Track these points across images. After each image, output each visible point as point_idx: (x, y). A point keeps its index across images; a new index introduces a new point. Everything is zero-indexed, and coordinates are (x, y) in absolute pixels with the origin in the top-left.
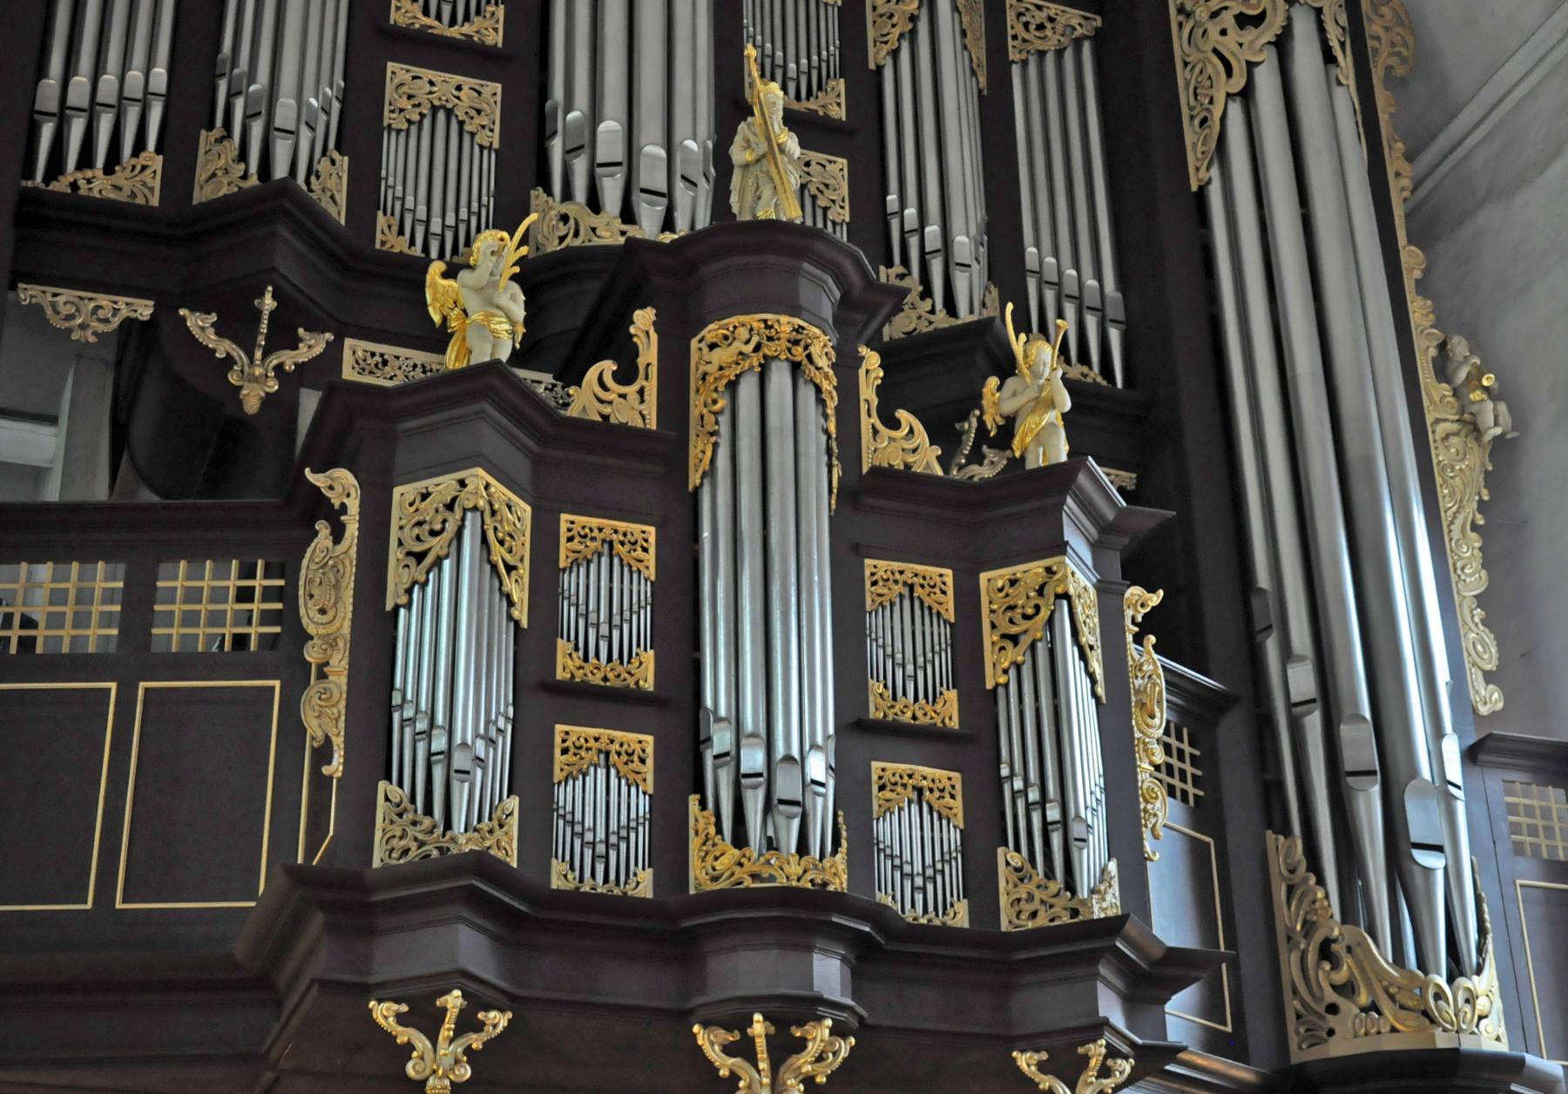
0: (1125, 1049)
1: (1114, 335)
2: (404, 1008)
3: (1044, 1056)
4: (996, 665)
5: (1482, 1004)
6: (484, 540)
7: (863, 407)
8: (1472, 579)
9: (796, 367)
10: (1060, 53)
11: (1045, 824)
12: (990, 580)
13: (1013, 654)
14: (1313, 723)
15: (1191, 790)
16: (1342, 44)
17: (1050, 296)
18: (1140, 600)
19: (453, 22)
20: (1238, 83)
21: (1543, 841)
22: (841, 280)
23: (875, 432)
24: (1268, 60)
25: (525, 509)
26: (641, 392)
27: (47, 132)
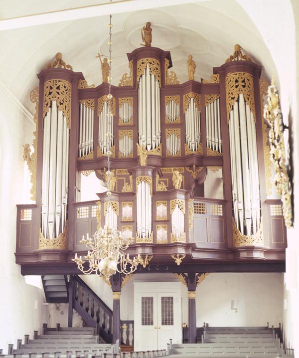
16: (248, 98)
24: (236, 103)
25: (118, 203)
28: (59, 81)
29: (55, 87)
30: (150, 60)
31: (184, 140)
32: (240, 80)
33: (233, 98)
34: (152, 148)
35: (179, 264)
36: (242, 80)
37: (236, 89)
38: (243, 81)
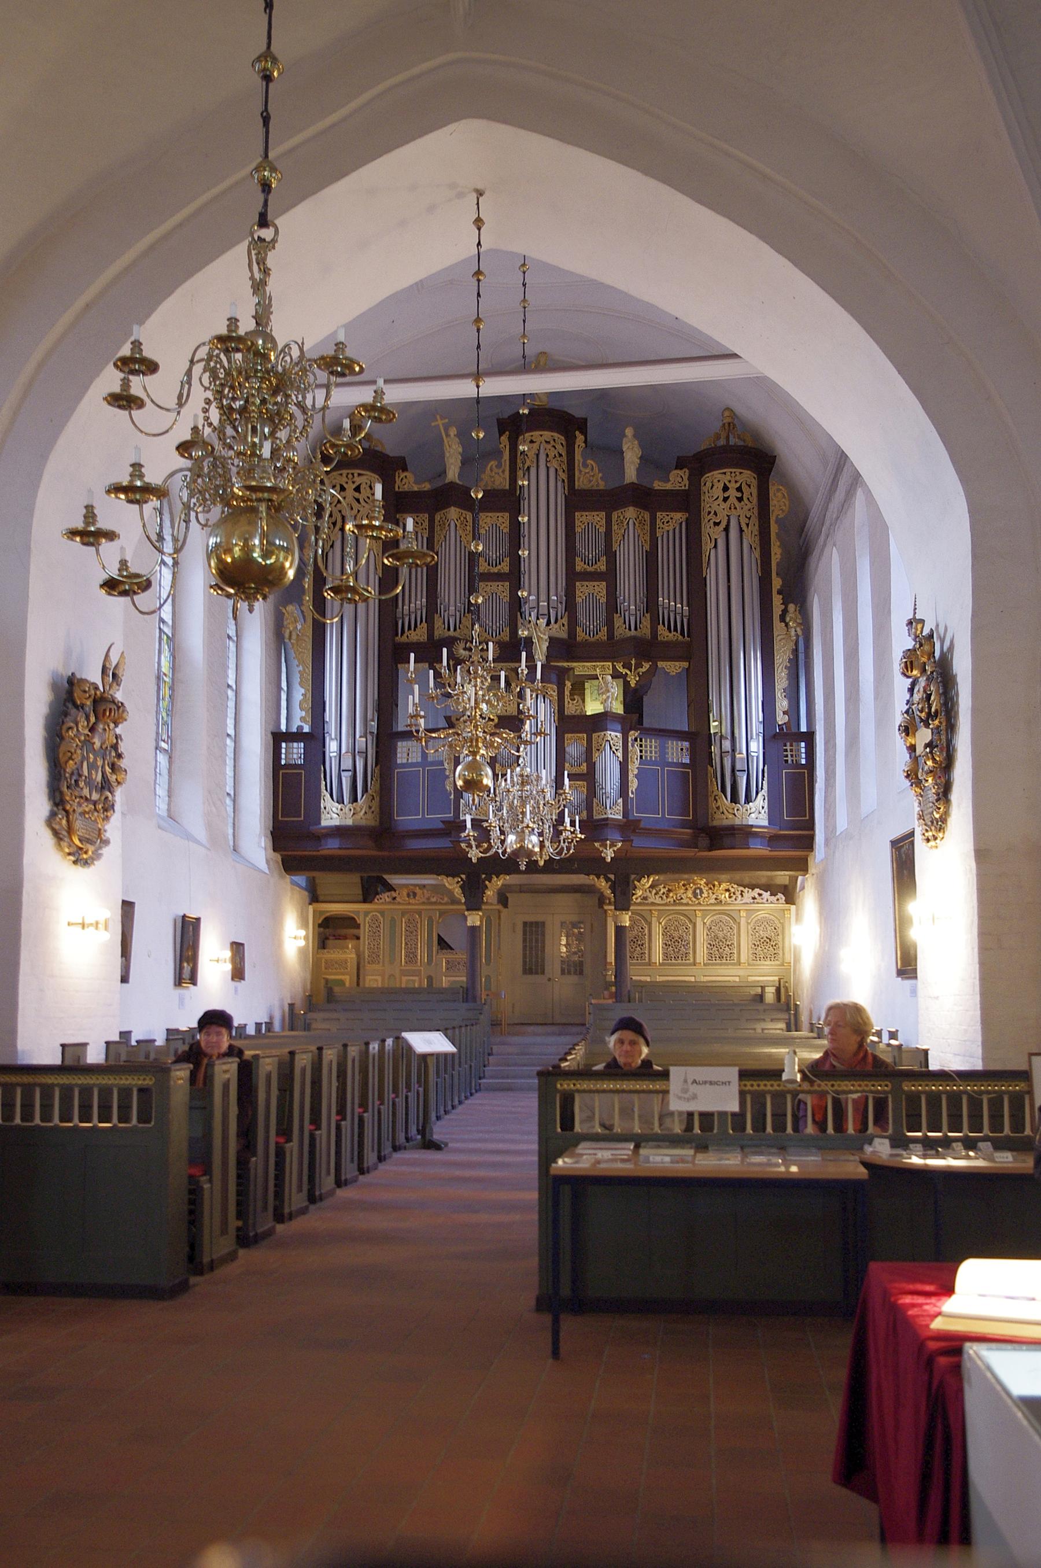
1: (685, 620)
16: (748, 525)
24: (724, 533)
28: (359, 475)
29: (350, 487)
30: (547, 435)
31: (612, 606)
32: (733, 486)
33: (716, 524)
34: (548, 623)
35: (609, 860)
36: (738, 485)
37: (723, 505)
38: (739, 489)
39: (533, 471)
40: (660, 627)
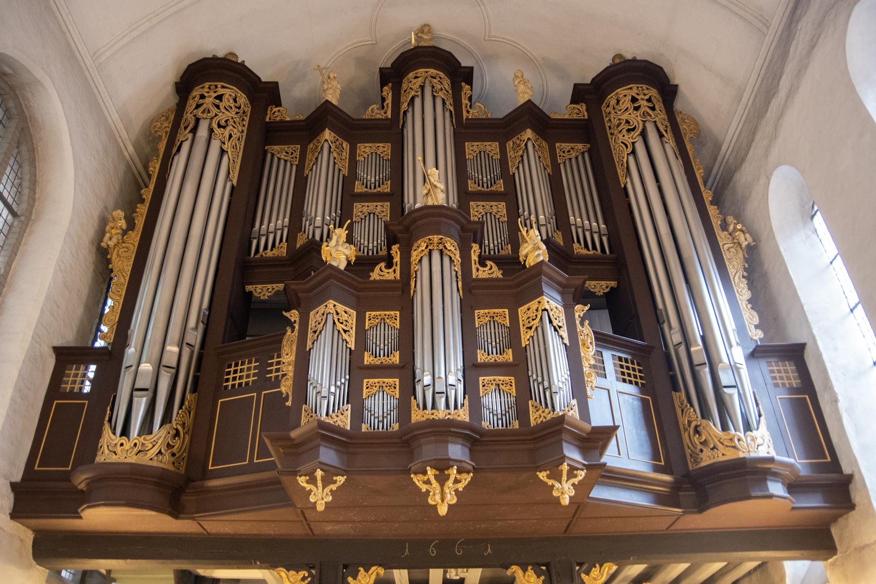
0: (580, 466)
1: (605, 239)
2: (308, 478)
3: (548, 472)
4: (525, 338)
5: (759, 441)
6: (334, 323)
7: (473, 262)
8: (743, 294)
9: (441, 252)
10: (577, 158)
11: (544, 390)
12: (521, 310)
13: (531, 333)
14: (682, 349)
15: (639, 381)
16: (666, 131)
17: (580, 230)
18: (580, 310)
19: (375, 188)
20: (630, 150)
21: (786, 381)
22: (457, 221)
23: (478, 270)
24: (640, 139)
26: (394, 271)
27: (255, 242)
28: (223, 87)
30: (432, 71)
33: (629, 131)
35: (565, 501)
36: (647, 97)
38: (649, 100)
39: (418, 102)
40: (576, 245)
